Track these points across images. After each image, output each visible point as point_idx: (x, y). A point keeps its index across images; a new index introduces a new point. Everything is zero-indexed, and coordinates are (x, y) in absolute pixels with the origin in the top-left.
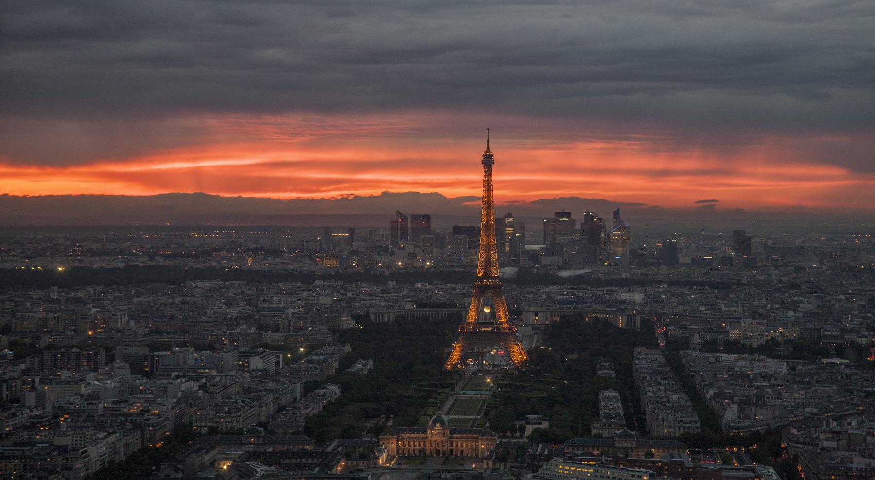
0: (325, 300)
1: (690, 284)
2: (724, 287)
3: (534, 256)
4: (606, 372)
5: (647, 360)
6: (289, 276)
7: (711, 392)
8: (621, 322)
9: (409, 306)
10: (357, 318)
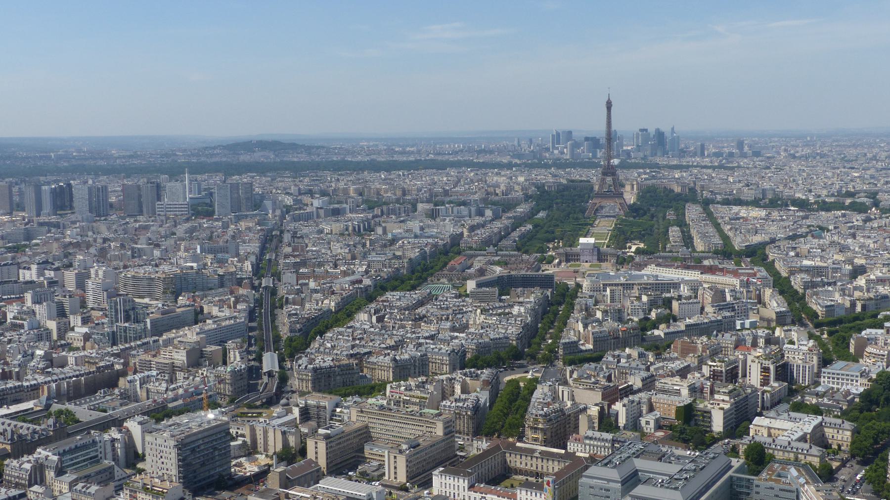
0: (521, 179)
1: (714, 168)
2: (732, 168)
3: (628, 153)
4: (671, 215)
5: (693, 212)
6: (500, 166)
7: (729, 227)
8: (677, 189)
9: (564, 182)
10: (538, 187)
